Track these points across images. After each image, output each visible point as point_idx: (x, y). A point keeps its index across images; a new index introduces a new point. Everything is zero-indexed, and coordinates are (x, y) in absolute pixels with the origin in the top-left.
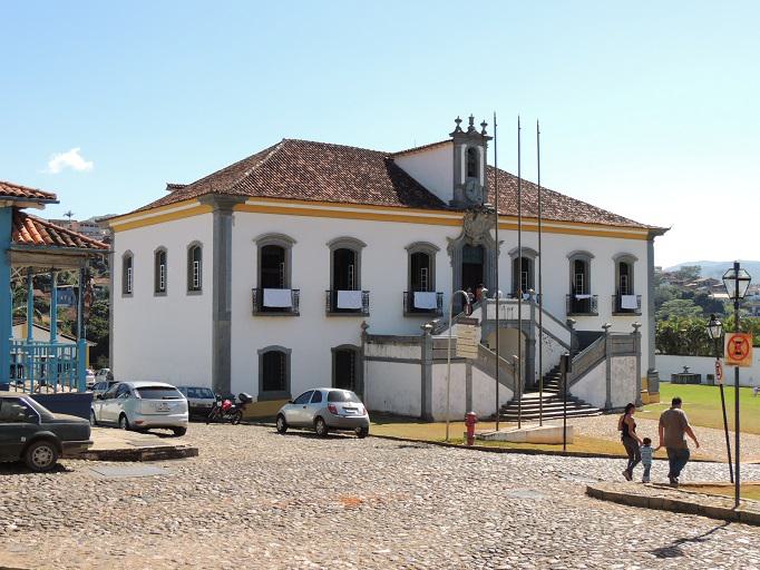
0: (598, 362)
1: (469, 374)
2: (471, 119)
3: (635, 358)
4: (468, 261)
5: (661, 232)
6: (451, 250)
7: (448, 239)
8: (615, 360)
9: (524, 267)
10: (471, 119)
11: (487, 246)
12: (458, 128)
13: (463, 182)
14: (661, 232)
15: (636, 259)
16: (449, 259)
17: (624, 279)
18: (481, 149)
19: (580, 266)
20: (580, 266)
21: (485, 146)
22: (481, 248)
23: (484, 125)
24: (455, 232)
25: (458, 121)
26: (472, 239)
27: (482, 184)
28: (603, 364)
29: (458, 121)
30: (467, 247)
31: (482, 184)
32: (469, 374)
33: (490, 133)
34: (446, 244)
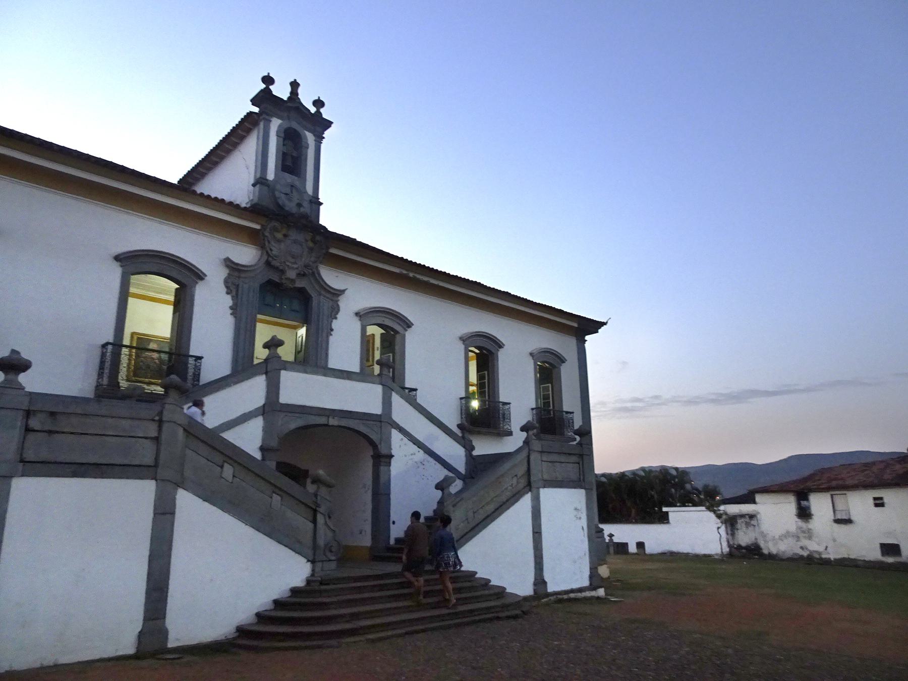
0: (515, 498)
1: (164, 513)
5: (593, 326)
10: (295, 85)
13: (271, 176)
14: (593, 326)
16: (228, 301)
17: (546, 389)
18: (310, 138)
21: (320, 138)
23: (319, 103)
26: (283, 272)
28: (526, 501)
29: (268, 80)
31: (309, 189)
32: (164, 513)
33: (326, 113)
34: (223, 273)
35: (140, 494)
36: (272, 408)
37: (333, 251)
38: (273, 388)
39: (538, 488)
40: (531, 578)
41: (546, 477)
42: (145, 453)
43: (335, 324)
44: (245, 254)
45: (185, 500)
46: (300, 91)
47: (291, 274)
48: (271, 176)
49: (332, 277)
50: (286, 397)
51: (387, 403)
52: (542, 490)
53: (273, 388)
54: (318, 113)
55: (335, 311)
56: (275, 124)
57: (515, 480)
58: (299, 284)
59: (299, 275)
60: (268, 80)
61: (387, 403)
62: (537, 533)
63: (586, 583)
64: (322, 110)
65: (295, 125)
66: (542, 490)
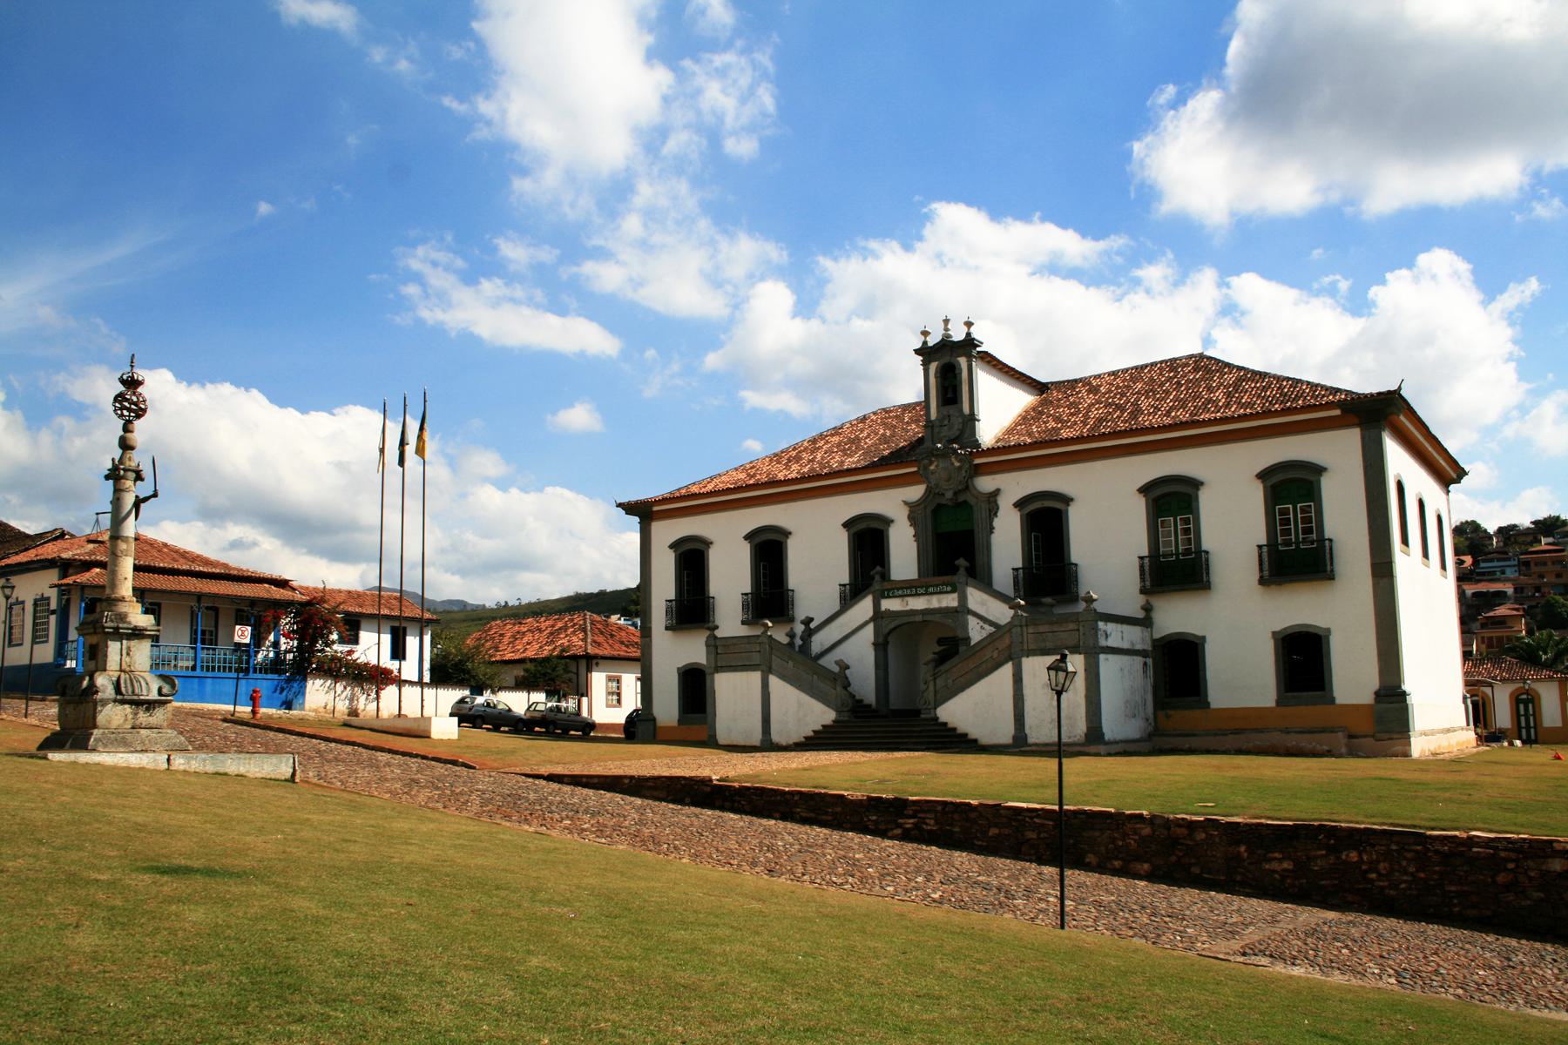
0: (998, 665)
2: (946, 321)
6: (914, 510)
7: (906, 503)
9: (1046, 522)
10: (946, 321)
11: (972, 501)
12: (925, 343)
13: (933, 415)
15: (1319, 470)
16: (911, 531)
18: (963, 361)
23: (969, 324)
24: (916, 492)
25: (925, 333)
28: (1007, 670)
29: (925, 333)
30: (938, 510)
31: (966, 410)
36: (878, 616)
37: (977, 461)
38: (876, 605)
39: (1020, 658)
41: (1032, 647)
42: (756, 659)
43: (996, 523)
44: (916, 492)
48: (933, 415)
49: (985, 483)
51: (963, 599)
52: (1024, 660)
54: (968, 334)
55: (993, 510)
56: (933, 366)
57: (995, 654)
58: (961, 499)
59: (955, 494)
65: (946, 359)
66: (1024, 660)
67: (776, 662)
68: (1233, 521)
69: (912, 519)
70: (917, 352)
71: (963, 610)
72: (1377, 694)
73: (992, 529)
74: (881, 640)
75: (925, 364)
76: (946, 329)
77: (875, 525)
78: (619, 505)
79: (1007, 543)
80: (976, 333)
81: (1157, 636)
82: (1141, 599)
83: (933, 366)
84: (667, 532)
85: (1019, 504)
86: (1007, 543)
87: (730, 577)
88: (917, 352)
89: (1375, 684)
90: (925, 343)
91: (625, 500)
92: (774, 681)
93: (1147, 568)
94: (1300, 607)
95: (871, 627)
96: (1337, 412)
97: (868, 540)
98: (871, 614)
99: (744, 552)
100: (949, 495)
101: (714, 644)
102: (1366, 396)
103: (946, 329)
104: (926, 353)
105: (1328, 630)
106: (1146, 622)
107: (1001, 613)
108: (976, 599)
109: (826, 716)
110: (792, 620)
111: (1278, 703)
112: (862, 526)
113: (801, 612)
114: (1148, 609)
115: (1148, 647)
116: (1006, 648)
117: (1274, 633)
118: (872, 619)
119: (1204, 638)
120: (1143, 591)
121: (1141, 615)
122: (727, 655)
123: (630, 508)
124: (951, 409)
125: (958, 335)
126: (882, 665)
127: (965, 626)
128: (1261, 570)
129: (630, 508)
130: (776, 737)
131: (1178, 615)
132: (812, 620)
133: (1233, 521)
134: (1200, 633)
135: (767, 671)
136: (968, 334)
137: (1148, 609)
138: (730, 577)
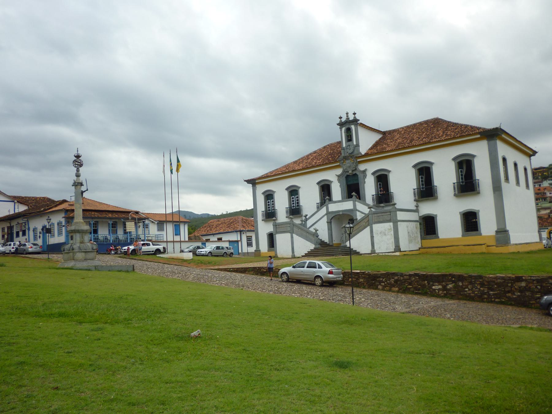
1: (292, 237)
2: (347, 114)
3: (391, 224)
4: (350, 183)
8: (376, 227)
9: (382, 179)
10: (347, 114)
11: (358, 173)
12: (341, 121)
16: (339, 184)
18: (353, 127)
19: (425, 172)
20: (425, 172)
22: (356, 175)
23: (354, 114)
24: (339, 171)
25: (341, 118)
27: (355, 143)
28: (368, 229)
30: (347, 177)
31: (355, 143)
32: (292, 237)
34: (337, 178)
35: (288, 235)
36: (328, 213)
37: (358, 160)
38: (327, 209)
40: (370, 248)
42: (289, 229)
43: (366, 180)
44: (339, 171)
45: (294, 235)
46: (349, 115)
47: (350, 172)
49: (362, 167)
50: (330, 210)
51: (355, 205)
52: (374, 225)
53: (327, 209)
54: (355, 117)
55: (365, 176)
56: (344, 129)
58: (354, 173)
59: (353, 171)
60: (341, 118)
61: (355, 205)
62: (372, 237)
63: (393, 251)
64: (356, 115)
65: (347, 126)
66: (374, 225)
67: (295, 229)
68: (445, 176)
69: (339, 181)
70: (338, 124)
71: (355, 210)
72: (496, 232)
73: (365, 182)
74: (329, 221)
75: (341, 129)
76: (347, 116)
77: (327, 183)
78: (245, 181)
79: (370, 188)
80: (358, 117)
81: (421, 215)
82: (415, 203)
83: (344, 129)
84: (261, 188)
85: (373, 174)
86: (370, 188)
87: (282, 203)
88: (338, 124)
89: (495, 228)
90: (341, 121)
91: (247, 179)
92: (294, 235)
93: (416, 192)
94: (469, 204)
95: (326, 216)
96: (479, 136)
97: (325, 189)
98: (325, 212)
99: (286, 194)
100: (350, 172)
101: (276, 226)
102: (490, 130)
103: (347, 116)
104: (341, 125)
105: (479, 211)
106: (417, 211)
107: (366, 210)
108: (360, 206)
109: (311, 246)
110: (302, 216)
111: (463, 236)
112: (323, 184)
113: (304, 213)
114: (417, 206)
115: (417, 219)
116: (368, 221)
117: (460, 213)
118: (326, 214)
119: (436, 215)
120: (415, 200)
121: (415, 208)
122: (280, 228)
123: (248, 181)
124: (350, 143)
125: (351, 118)
126: (330, 229)
127: (356, 215)
128: (455, 191)
129: (248, 181)
130: (297, 254)
131: (427, 208)
132: (307, 215)
133: (445, 176)
134: (435, 214)
135: (292, 233)
136: (355, 117)
137: (417, 207)
138: (282, 203)
